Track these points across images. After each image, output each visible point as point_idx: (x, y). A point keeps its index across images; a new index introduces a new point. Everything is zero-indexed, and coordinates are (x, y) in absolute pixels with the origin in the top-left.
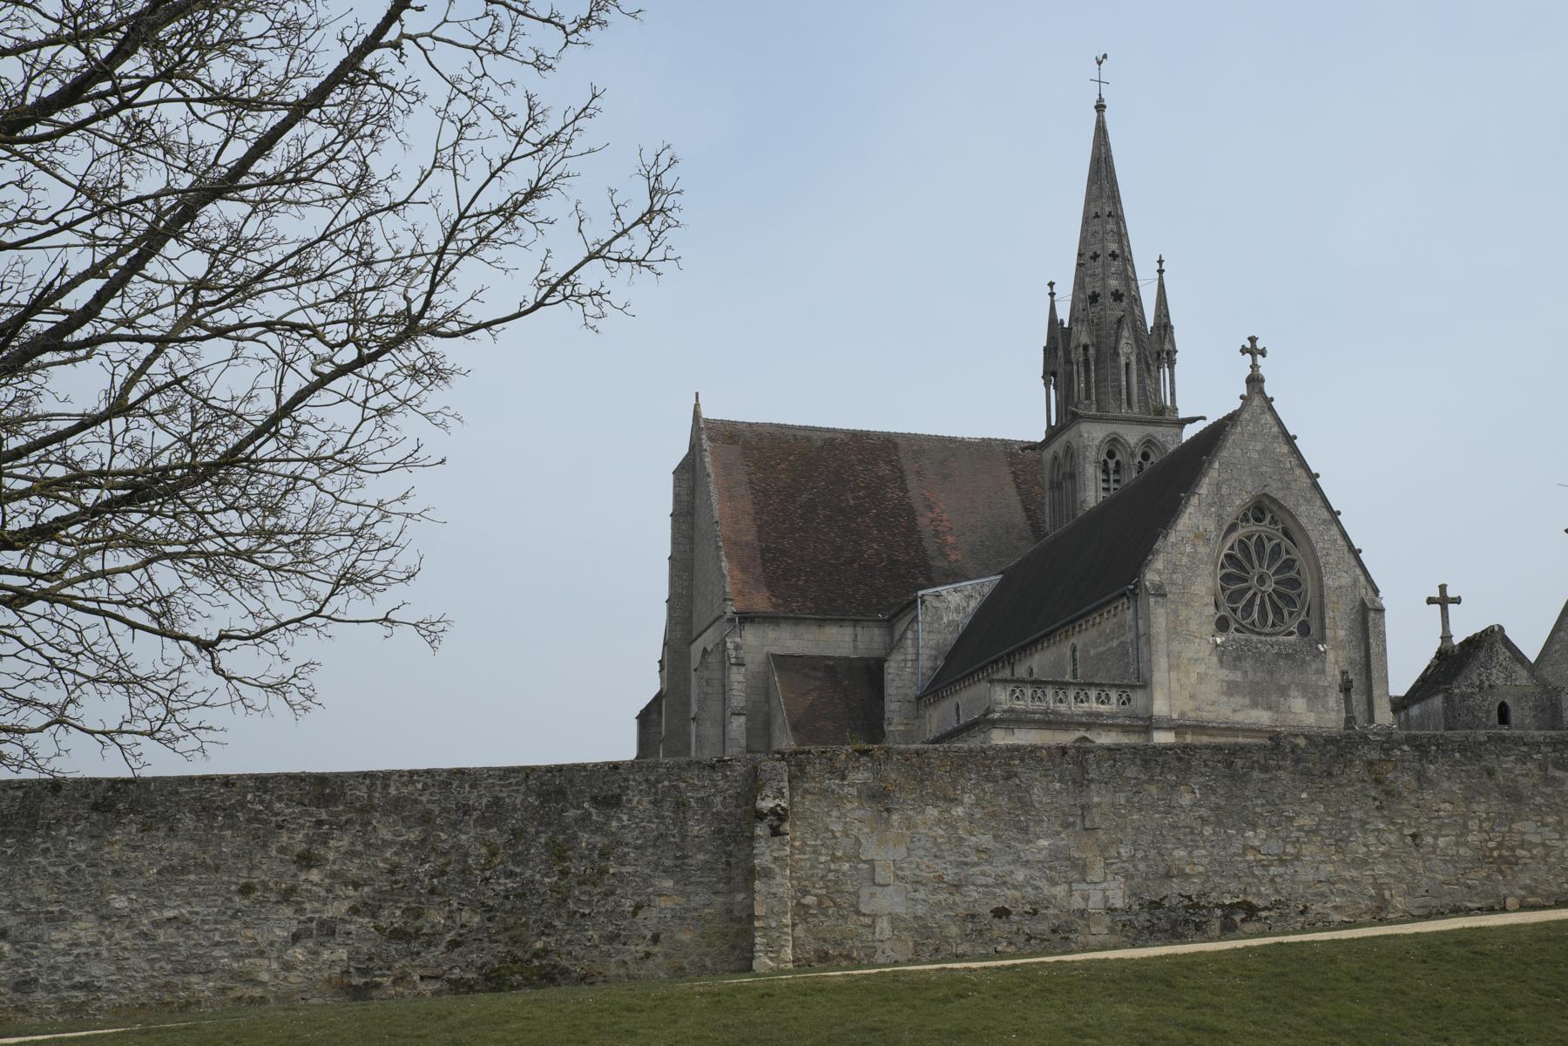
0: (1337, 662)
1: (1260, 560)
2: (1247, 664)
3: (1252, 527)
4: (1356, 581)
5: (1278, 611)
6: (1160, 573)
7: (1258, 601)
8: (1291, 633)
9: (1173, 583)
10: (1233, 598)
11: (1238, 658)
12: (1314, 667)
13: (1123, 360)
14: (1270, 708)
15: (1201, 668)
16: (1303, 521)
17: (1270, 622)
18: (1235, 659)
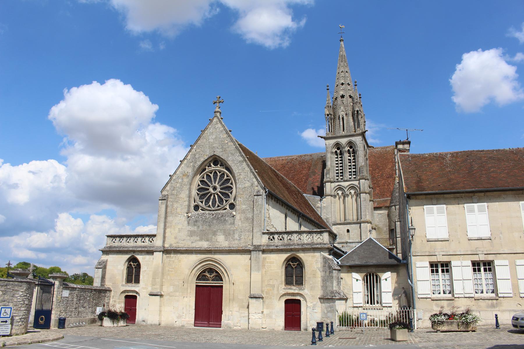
1: (211, 181)
2: (199, 224)
3: (213, 167)
4: (252, 184)
8: (226, 209)
9: (172, 194)
10: (201, 197)
11: (196, 221)
12: (229, 222)
13: (341, 117)
14: (208, 240)
15: (180, 226)
17: (217, 205)
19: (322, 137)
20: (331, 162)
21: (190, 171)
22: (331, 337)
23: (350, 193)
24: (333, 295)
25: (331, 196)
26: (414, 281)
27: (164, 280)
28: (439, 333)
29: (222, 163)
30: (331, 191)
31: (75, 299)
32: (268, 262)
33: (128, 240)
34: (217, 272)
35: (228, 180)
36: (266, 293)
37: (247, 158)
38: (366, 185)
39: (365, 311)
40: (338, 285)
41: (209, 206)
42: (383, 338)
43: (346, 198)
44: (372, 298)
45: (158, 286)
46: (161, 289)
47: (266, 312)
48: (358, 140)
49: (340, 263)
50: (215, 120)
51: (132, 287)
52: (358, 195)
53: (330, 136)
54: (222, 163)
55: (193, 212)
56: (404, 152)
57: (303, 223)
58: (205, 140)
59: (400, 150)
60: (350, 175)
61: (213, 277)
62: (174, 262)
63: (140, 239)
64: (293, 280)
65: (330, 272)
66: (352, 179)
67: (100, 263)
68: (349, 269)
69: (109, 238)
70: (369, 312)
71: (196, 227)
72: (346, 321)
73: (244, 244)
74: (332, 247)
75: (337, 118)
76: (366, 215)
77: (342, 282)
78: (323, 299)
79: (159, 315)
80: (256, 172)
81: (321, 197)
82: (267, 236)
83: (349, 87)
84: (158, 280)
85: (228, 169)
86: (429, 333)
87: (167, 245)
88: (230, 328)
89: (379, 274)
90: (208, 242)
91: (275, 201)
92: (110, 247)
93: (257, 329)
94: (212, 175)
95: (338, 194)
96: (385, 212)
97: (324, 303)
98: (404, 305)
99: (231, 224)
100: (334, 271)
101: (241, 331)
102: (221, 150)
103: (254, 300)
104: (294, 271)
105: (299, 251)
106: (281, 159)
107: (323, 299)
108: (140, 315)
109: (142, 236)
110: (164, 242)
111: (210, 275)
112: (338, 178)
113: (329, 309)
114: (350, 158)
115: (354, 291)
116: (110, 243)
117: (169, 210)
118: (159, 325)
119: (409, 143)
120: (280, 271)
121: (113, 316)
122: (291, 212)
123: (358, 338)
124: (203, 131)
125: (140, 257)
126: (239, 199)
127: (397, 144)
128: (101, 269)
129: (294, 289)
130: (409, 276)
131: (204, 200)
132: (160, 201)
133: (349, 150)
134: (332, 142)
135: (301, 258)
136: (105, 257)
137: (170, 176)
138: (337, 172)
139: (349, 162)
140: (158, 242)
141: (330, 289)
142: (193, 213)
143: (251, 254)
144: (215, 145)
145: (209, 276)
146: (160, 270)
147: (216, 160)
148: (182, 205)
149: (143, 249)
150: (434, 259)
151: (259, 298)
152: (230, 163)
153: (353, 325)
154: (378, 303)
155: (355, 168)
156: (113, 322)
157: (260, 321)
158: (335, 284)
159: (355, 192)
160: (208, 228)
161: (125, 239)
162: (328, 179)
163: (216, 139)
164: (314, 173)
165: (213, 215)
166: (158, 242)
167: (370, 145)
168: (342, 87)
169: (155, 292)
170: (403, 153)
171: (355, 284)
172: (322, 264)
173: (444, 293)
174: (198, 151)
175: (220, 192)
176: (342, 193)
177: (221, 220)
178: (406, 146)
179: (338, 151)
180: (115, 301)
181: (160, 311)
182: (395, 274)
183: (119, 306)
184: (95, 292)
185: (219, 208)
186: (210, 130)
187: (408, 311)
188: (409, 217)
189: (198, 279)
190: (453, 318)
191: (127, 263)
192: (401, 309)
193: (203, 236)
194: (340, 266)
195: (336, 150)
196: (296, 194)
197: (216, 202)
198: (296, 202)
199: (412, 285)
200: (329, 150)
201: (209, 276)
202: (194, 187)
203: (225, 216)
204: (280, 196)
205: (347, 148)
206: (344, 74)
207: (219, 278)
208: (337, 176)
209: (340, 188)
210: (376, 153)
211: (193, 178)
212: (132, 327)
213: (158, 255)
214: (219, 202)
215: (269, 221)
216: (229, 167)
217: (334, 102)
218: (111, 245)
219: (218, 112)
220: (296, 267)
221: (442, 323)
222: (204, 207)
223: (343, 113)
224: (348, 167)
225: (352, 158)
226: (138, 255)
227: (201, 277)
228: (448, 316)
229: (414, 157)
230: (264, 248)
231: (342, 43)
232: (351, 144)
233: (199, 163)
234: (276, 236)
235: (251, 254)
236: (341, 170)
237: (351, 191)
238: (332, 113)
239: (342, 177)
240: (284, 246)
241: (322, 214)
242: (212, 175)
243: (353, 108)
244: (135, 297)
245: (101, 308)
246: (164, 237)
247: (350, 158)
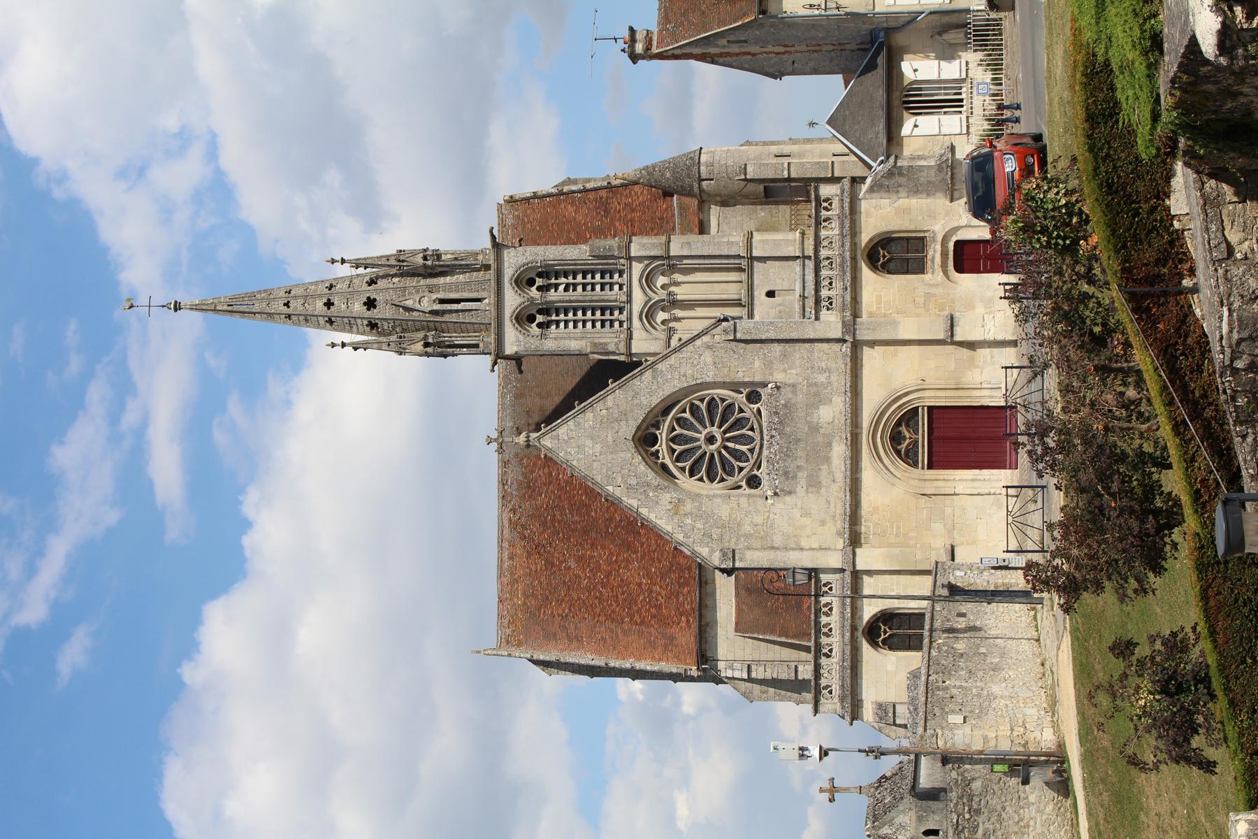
0: (785, 371)
2: (792, 466)
3: (662, 446)
4: (709, 347)
5: (739, 423)
7: (731, 445)
8: (759, 411)
9: (721, 539)
11: (786, 474)
12: (790, 395)
13: (437, 307)
14: (830, 444)
15: (797, 513)
16: (655, 400)
17: (750, 433)
18: (787, 479)
23: (663, 287)
26: (919, 9)
32: (878, 308)
34: (898, 424)
35: (694, 410)
41: (752, 451)
43: (679, 297)
56: (651, 40)
58: (595, 464)
62: (876, 524)
69: (821, 708)
71: (800, 474)
73: (840, 361)
75: (438, 319)
76: (729, 243)
82: (824, 312)
90: (835, 444)
92: (842, 699)
94: (679, 448)
99: (794, 392)
102: (623, 423)
106: (506, 565)
111: (905, 438)
114: (562, 288)
125: (869, 610)
126: (740, 374)
129: (934, 252)
130: (909, 20)
131: (736, 464)
136: (868, 712)
141: (932, 172)
144: (610, 439)
145: (908, 441)
147: (645, 440)
148: (747, 513)
160: (802, 445)
165: (772, 437)
171: (924, 133)
172: (884, 195)
177: (783, 416)
189: (915, 465)
194: (888, 157)
201: (908, 441)
205: (533, 292)
209: (649, 314)
216: (663, 406)
218: (836, 700)
222: (752, 461)
223: (425, 300)
225: (563, 280)
226: (861, 618)
227: (909, 457)
232: (524, 281)
234: (824, 293)
237: (659, 285)
238: (421, 335)
240: (844, 272)
242: (679, 448)
247: (562, 288)
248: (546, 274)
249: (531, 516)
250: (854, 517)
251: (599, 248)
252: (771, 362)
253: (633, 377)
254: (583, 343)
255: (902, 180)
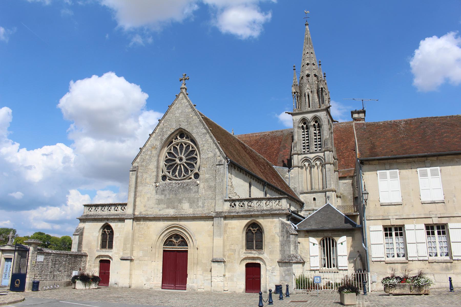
0: (204, 188)
1: (177, 153)
2: (166, 192)
3: (179, 140)
5: (186, 171)
6: (138, 163)
7: (178, 167)
9: (142, 166)
10: (169, 168)
11: (164, 190)
12: (194, 190)
13: (306, 94)
14: (174, 208)
15: (149, 195)
17: (183, 175)
18: (162, 191)
19: (289, 114)
20: (299, 135)
21: (158, 144)
22: (284, 300)
23: (316, 164)
24: (290, 259)
25: (299, 167)
26: (368, 245)
27: (134, 245)
28: (391, 296)
29: (187, 136)
30: (298, 163)
31: (50, 264)
33: (103, 209)
34: (182, 238)
35: (193, 152)
36: (228, 257)
37: (211, 130)
38: (331, 156)
39: (321, 275)
40: (295, 249)
41: (176, 176)
42: (333, 301)
43: (312, 169)
44: (329, 260)
45: (128, 252)
46: (132, 254)
47: (227, 275)
48: (322, 115)
49: (297, 228)
50: (181, 95)
51: (105, 252)
52: (323, 165)
53: (297, 112)
54: (187, 136)
55: (162, 182)
56: (360, 120)
57: (269, 191)
58: (172, 115)
59: (355, 119)
60: (315, 147)
61: (179, 242)
62: (143, 228)
63: (113, 207)
64: (253, 245)
65: (288, 237)
66: (318, 151)
67: (77, 231)
68: (307, 234)
69: (86, 207)
70: (326, 275)
71: (163, 196)
72: (303, 283)
74: (290, 213)
75: (303, 95)
76: (330, 184)
77: (300, 246)
78: (282, 263)
79: (130, 279)
80: (219, 143)
81: (289, 168)
82: (229, 203)
83: (314, 67)
84: (129, 246)
85: (193, 141)
86: (380, 297)
87: (137, 213)
88: (194, 290)
89: (335, 238)
90: (174, 210)
91: (238, 170)
92: (87, 215)
93: (219, 291)
94: (178, 147)
95: (305, 165)
96: (349, 181)
97: (282, 266)
98: (360, 268)
99: (195, 192)
100: (291, 236)
101: (203, 293)
103: (216, 264)
104: (254, 236)
105: (258, 217)
107: (282, 263)
108: (112, 279)
109: (115, 205)
110: (134, 210)
111: (177, 240)
112: (304, 150)
113: (287, 272)
114: (315, 132)
115: (311, 255)
116: (87, 211)
117: (139, 180)
118: (130, 287)
119: (364, 112)
120: (241, 236)
121: (85, 279)
122: (256, 181)
123: (309, 302)
124: (170, 107)
125: (112, 225)
126: (203, 169)
127: (353, 113)
128: (78, 236)
129: (254, 254)
130: (364, 240)
132: (131, 172)
133: (314, 125)
134: (299, 117)
135: (260, 224)
136: (82, 225)
137: (140, 149)
138: (304, 145)
139: (315, 136)
140: (129, 210)
141: (288, 253)
142: (161, 183)
143: (213, 221)
144: (181, 119)
145: (175, 241)
146: (131, 236)
147: (182, 133)
148: (150, 175)
149: (116, 217)
150: (387, 223)
151: (221, 262)
152: (194, 135)
153: (309, 288)
154: (334, 266)
155: (320, 141)
156: (85, 285)
157: (221, 284)
158: (292, 248)
159: (320, 163)
160: (174, 196)
161: (100, 208)
162: (296, 152)
163: (183, 113)
164: (284, 147)
165: (179, 184)
166: (129, 210)
167: (334, 120)
168: (308, 67)
169: (126, 256)
170: (358, 122)
171: (312, 247)
172: (280, 229)
173: (398, 256)
174: (165, 125)
175: (185, 163)
176: (309, 165)
178: (362, 115)
179: (305, 126)
180: (91, 266)
181: (131, 275)
182: (350, 239)
183: (94, 270)
184: (71, 257)
185: (185, 177)
186: (177, 105)
187: (363, 274)
188: (363, 182)
189: (165, 244)
190: (406, 282)
191: (102, 230)
192: (356, 272)
193: (170, 204)
194: (297, 231)
195: (303, 124)
196: (264, 165)
197: (182, 172)
198: (262, 173)
199: (366, 248)
200: (296, 125)
201: (175, 241)
202: (162, 159)
203: (190, 185)
204: (244, 166)
205: (313, 123)
206: (309, 55)
207: (184, 243)
208: (304, 149)
209: (307, 160)
210: (342, 128)
211: (161, 150)
212: (103, 289)
213: (129, 222)
214: (185, 172)
215: (232, 189)
216: (194, 139)
217: (300, 81)
218: (88, 213)
219: (183, 88)
220: (256, 232)
221: (394, 286)
222: (171, 177)
223: (309, 90)
224: (314, 140)
225: (317, 132)
226: (111, 222)
227: (168, 242)
228: (400, 279)
229: (368, 125)
230: (226, 214)
231: (307, 27)
232: (316, 119)
233: (166, 136)
234: (237, 203)
235: (213, 221)
236: (307, 143)
237: (317, 162)
238: (298, 91)
239: (308, 150)
240: (245, 212)
241: (290, 184)
242: (178, 147)
243: (318, 86)
244: (108, 262)
245: (77, 272)
246: (135, 205)
247: (315, 132)
248: (318, 126)
249: (266, 140)
250: (146, 219)
251: (327, 141)
252: (208, 181)
253: (204, 125)
254: (297, 140)
255: (285, 237)
